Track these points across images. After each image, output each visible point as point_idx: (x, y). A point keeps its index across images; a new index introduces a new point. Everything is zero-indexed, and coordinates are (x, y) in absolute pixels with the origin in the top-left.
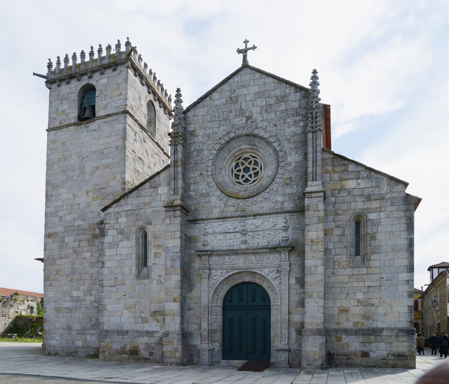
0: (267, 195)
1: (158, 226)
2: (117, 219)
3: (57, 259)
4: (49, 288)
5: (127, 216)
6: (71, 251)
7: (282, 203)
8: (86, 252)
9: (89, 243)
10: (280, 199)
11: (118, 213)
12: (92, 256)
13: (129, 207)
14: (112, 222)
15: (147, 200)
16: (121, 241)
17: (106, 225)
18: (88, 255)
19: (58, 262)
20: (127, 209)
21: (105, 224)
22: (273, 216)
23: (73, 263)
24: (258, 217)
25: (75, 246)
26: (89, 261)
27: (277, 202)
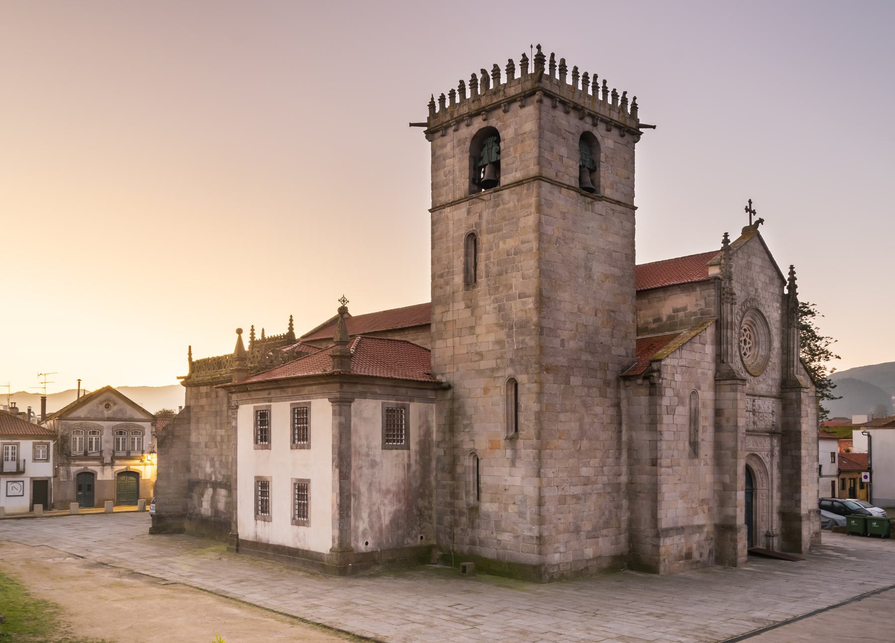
0: (765, 377)
1: (705, 393)
2: (674, 374)
3: (559, 412)
4: (549, 461)
5: (682, 373)
6: (578, 402)
7: (772, 386)
8: (598, 405)
9: (600, 391)
10: (770, 382)
11: (674, 366)
12: (604, 413)
13: (684, 363)
14: (669, 378)
15: (697, 357)
16: (677, 405)
17: (664, 381)
18: (598, 410)
19: (562, 417)
20: (681, 364)
21: (663, 379)
22: (768, 399)
23: (580, 420)
24: (761, 398)
25: (584, 394)
26: (601, 421)
27: (768, 385)
